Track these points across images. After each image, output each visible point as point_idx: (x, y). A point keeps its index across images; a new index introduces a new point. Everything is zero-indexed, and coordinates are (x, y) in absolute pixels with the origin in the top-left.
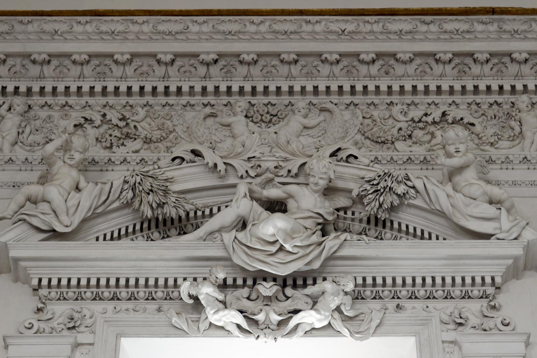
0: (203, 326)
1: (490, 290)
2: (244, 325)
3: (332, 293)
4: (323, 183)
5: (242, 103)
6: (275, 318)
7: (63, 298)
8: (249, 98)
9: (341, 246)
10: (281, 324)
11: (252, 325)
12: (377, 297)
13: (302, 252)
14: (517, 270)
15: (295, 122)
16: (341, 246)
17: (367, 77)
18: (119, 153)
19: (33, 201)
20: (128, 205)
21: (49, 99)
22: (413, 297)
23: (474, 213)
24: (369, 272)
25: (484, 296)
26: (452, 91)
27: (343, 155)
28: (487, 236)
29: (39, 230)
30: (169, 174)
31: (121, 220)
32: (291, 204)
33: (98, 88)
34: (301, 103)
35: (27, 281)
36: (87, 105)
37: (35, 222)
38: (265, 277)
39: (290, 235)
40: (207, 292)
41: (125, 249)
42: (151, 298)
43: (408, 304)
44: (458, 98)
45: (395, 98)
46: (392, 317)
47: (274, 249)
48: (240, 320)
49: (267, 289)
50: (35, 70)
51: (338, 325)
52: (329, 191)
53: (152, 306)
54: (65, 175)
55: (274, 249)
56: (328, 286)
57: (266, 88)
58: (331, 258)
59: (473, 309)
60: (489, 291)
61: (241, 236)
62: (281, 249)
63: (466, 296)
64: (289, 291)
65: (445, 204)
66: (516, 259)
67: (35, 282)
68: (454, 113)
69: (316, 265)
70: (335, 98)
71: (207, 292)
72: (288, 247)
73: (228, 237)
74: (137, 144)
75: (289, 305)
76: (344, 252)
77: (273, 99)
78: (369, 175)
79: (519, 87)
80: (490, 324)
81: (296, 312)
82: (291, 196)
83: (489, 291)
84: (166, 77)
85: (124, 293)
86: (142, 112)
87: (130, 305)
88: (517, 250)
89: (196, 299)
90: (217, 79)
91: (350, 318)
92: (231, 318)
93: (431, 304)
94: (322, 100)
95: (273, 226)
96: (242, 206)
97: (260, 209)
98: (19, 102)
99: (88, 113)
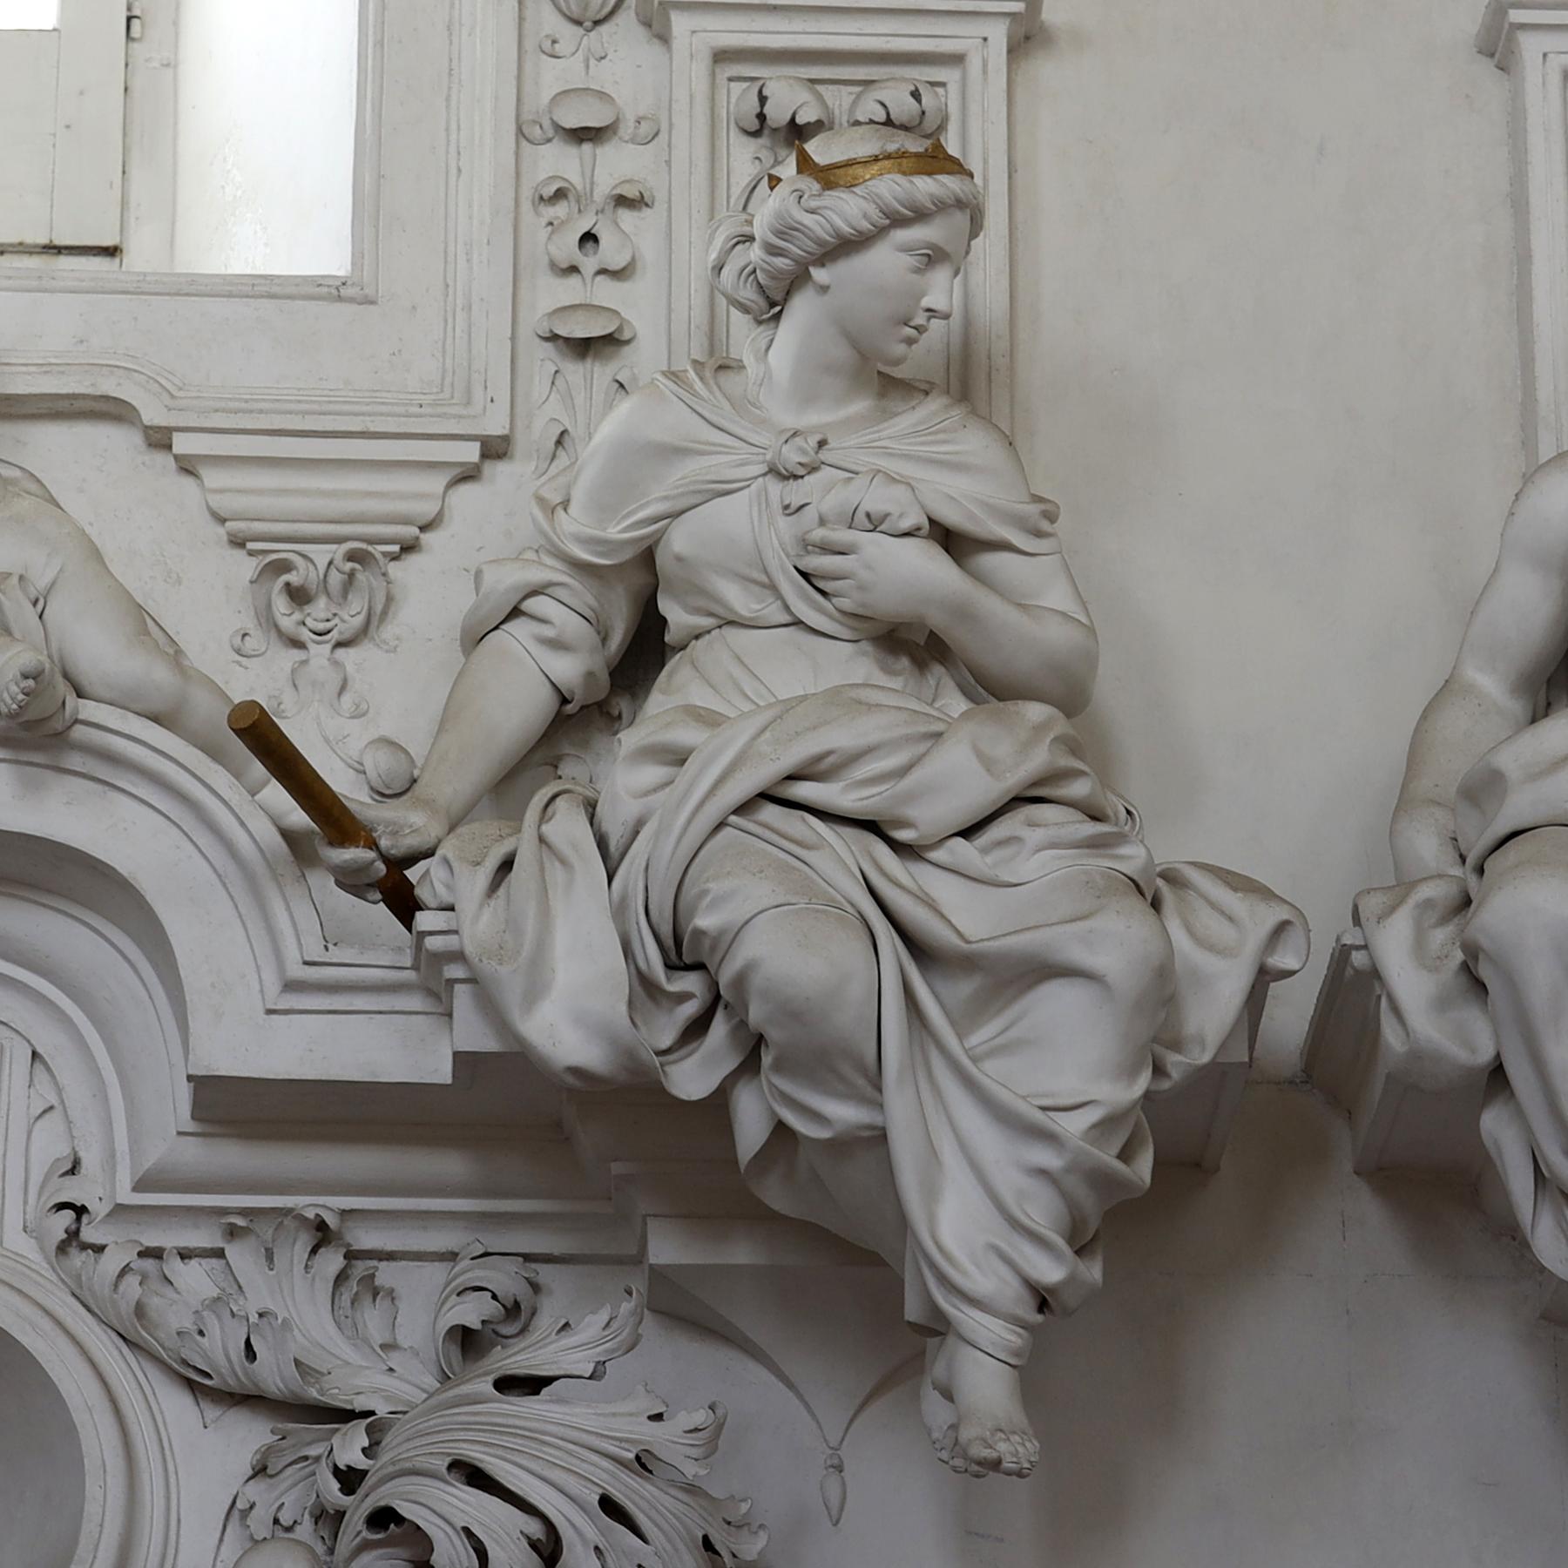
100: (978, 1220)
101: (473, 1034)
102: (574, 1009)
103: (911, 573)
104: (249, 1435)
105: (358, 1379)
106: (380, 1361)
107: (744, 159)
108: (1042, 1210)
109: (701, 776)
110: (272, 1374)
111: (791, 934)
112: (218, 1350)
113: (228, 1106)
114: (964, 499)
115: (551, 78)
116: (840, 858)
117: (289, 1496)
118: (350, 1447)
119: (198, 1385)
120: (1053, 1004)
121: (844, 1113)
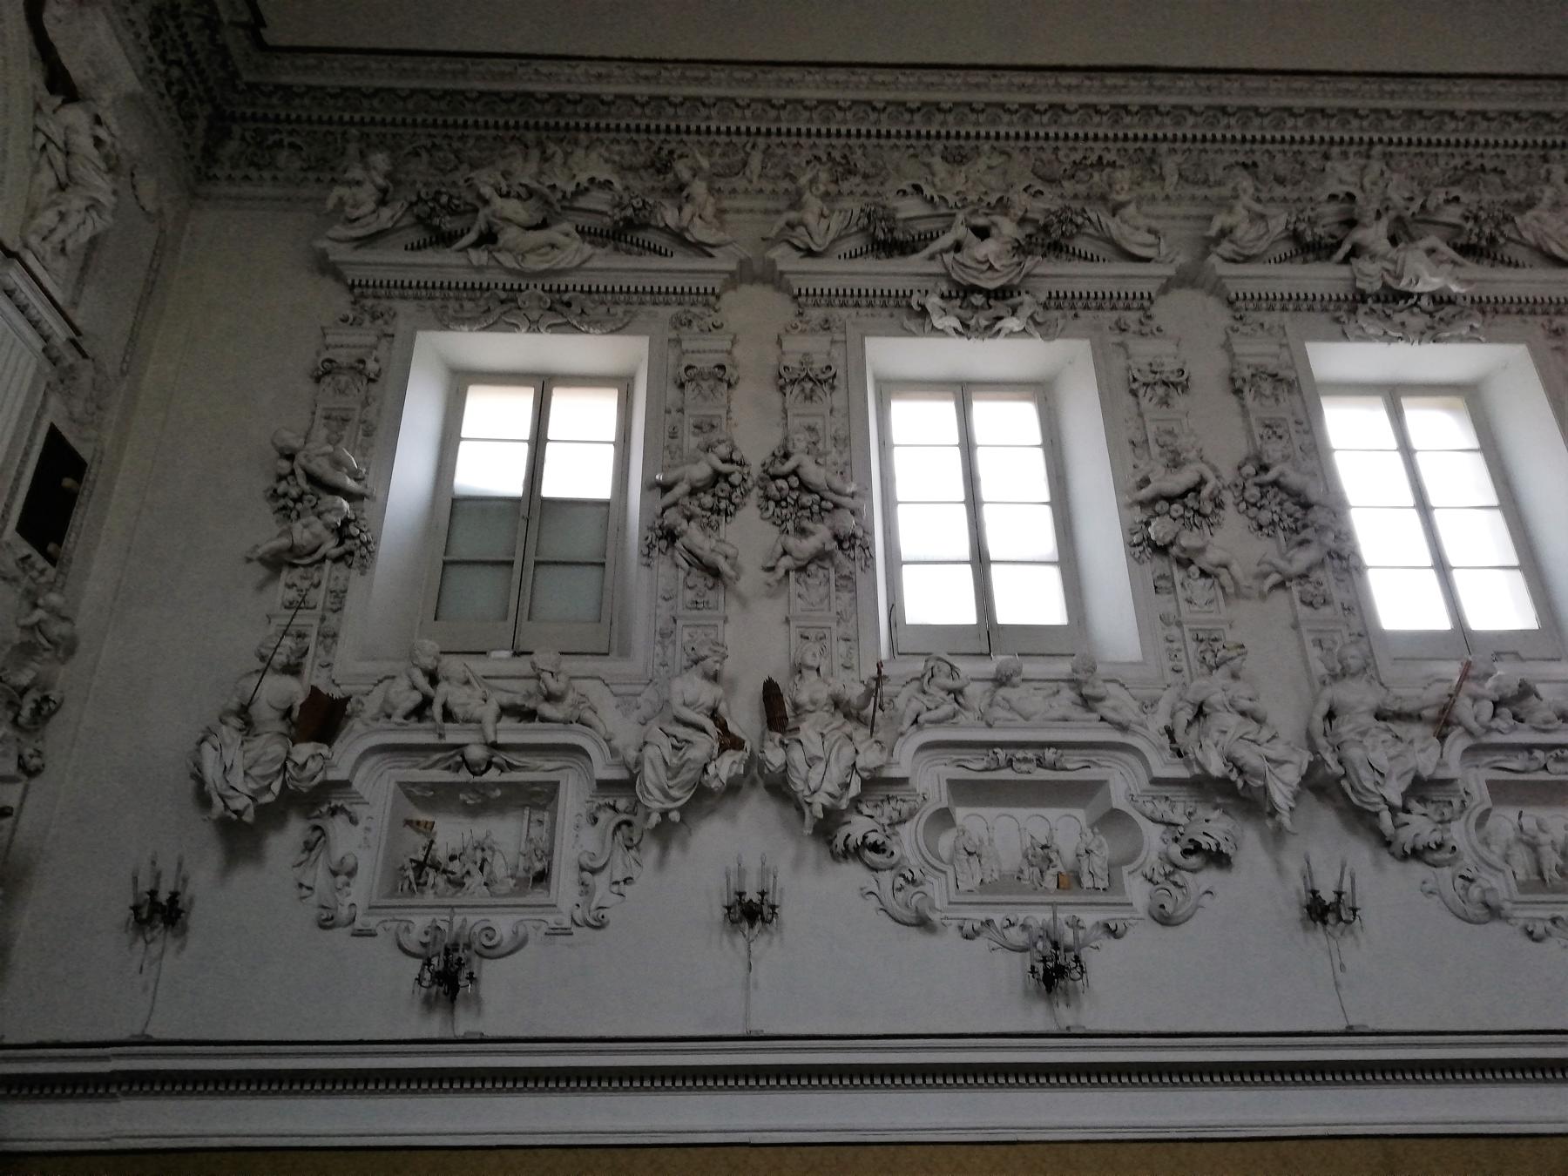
0: (928, 328)
1: (1146, 303)
2: (960, 328)
4: (1020, 213)
5: (939, 146)
6: (984, 323)
7: (817, 305)
10: (987, 328)
15: (982, 163)
16: (1035, 266)
17: (1041, 125)
18: (845, 186)
19: (791, 226)
20: (864, 229)
21: (784, 139)
22: (1086, 307)
23: (1136, 242)
25: (1142, 308)
27: (1032, 190)
28: (1148, 260)
29: (798, 248)
31: (854, 243)
32: (994, 231)
33: (824, 130)
34: (986, 147)
35: (788, 290)
37: (796, 242)
40: (933, 302)
41: (860, 265)
42: (884, 305)
43: (1082, 313)
44: (1110, 145)
49: (978, 300)
50: (773, 113)
51: (1032, 329)
52: (1022, 221)
53: (885, 312)
54: (813, 204)
55: (985, 267)
57: (859, 131)
58: (1028, 275)
59: (1132, 318)
61: (958, 256)
62: (991, 267)
63: (1128, 308)
64: (992, 302)
65: (1115, 233)
67: (796, 291)
71: (933, 302)
72: (997, 266)
73: (948, 258)
74: (858, 179)
75: (991, 313)
76: (1038, 271)
77: (962, 142)
78: (1054, 208)
80: (1146, 330)
81: (1000, 318)
82: (994, 224)
83: (1143, 304)
84: (878, 121)
85: (864, 302)
87: (869, 311)
88: (1170, 271)
89: (923, 307)
93: (1100, 313)
95: (988, 248)
96: (960, 231)
97: (971, 235)
98: (761, 141)
99: (816, 152)
100: (1281, 795)
101: (1197, 771)
102: (1216, 768)
103: (1245, 704)
104: (1162, 828)
105: (1176, 820)
106: (1178, 817)
107: (1194, 644)
108: (1290, 796)
109: (1229, 735)
110: (1166, 819)
111: (1250, 757)
112: (1157, 815)
113: (1156, 781)
115: (1166, 633)
116: (1254, 746)
117: (1169, 837)
118: (1181, 830)
119: (1153, 820)
120: (1286, 767)
121: (1260, 783)
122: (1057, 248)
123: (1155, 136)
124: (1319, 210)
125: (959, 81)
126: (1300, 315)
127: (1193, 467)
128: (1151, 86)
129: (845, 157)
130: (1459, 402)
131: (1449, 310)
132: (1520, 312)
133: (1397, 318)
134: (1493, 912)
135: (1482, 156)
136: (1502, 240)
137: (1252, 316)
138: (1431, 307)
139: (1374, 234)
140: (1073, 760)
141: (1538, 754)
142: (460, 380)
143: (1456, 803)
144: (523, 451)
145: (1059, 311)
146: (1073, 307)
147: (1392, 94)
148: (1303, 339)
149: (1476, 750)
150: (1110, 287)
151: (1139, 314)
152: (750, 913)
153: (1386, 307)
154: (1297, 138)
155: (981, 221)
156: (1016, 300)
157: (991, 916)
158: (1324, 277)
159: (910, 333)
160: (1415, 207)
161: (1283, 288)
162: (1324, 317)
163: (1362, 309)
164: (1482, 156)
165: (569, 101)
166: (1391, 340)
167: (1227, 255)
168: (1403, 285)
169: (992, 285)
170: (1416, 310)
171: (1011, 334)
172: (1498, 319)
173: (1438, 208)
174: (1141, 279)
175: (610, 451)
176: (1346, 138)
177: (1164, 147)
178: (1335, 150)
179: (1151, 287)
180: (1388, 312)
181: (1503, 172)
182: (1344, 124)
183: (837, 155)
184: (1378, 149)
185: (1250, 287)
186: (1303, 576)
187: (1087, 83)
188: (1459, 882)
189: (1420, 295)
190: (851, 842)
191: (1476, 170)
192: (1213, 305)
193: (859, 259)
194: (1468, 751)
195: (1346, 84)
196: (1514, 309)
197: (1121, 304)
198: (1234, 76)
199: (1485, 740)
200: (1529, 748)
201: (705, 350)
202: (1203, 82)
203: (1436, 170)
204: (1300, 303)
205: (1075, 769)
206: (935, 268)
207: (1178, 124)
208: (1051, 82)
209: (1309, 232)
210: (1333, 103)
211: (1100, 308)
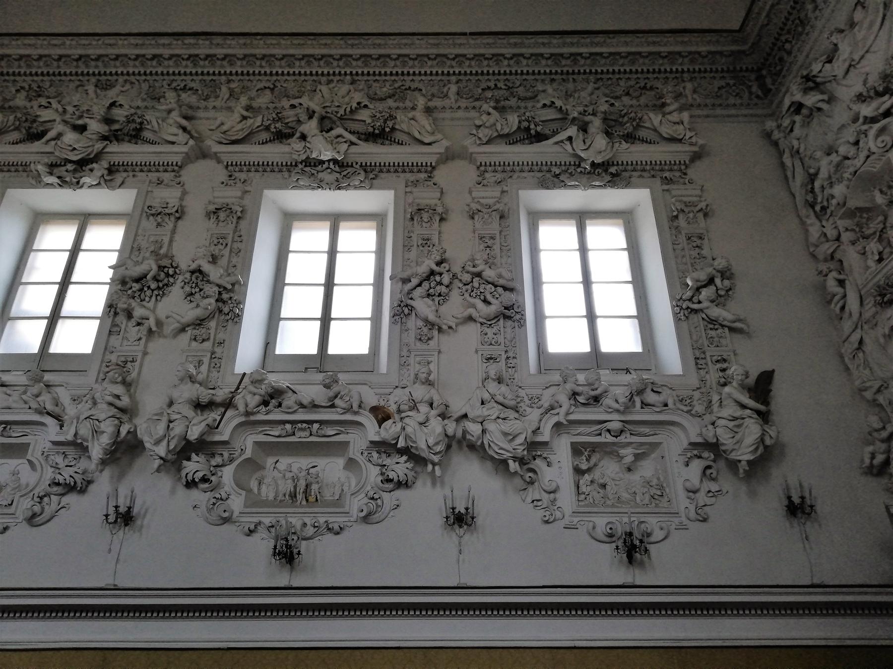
1: (176, 168)
3: (99, 169)
5: (93, 80)
8: (97, 77)
9: (103, 149)
11: (63, 183)
12: (125, 171)
13: (84, 150)
14: (188, 159)
22: (142, 171)
24: (116, 159)
25: (173, 171)
26: (191, 74)
28: (173, 143)
30: (38, 113)
34: (121, 79)
36: (24, 81)
38: (71, 162)
39: (78, 141)
45: (166, 77)
46: (130, 180)
47: (71, 148)
48: (57, 180)
49: (70, 167)
56: (94, 165)
59: (167, 177)
60: (177, 169)
61: (59, 143)
63: (166, 171)
66: (187, 153)
68: (192, 85)
69: (92, 156)
70: (138, 77)
73: (53, 143)
77: (109, 78)
79: (222, 72)
86: (48, 84)
87: (16, 174)
90: (83, 69)
91: (111, 180)
92: (53, 180)
93: (150, 174)
94: (132, 78)
103: (110, 399)
108: (101, 452)
113: (55, 443)
114: (117, 392)
122: (136, 135)
123: (220, 72)
124: (285, 113)
125: (100, 42)
126: (265, 174)
127: (146, 262)
128: (211, 43)
129: (39, 87)
130: (621, 221)
131: (349, 170)
132: (396, 171)
133: (321, 175)
134: (226, 521)
135: (413, 80)
136: (387, 130)
137: (237, 174)
138: (337, 169)
139: (311, 127)
140: (17, 431)
141: (288, 426)
142: (289, 220)
143: (226, 454)
144: (324, 258)
145: (113, 175)
146: (134, 171)
147: (352, 46)
148: (139, 189)
149: (248, 424)
150: (153, 159)
151: (173, 174)
152: (126, 518)
153: (309, 171)
154: (303, 72)
155: (80, 122)
156: (90, 166)
157: (263, 520)
158: (276, 152)
159: (33, 187)
160: (342, 112)
161: (253, 159)
162: (279, 175)
163: (298, 169)
164: (413, 80)
165: (238, 59)
166: (313, 189)
167: (217, 139)
168: (314, 156)
169: (75, 158)
170: (329, 170)
171: (91, 186)
172: (383, 175)
173: (352, 111)
174: (174, 154)
175: (372, 257)
176: (331, 72)
177: (223, 78)
178: (324, 79)
179: (178, 159)
180: (313, 172)
181: (421, 90)
182: (328, 64)
183: (34, 86)
184: (348, 77)
185: (236, 159)
186: (199, 323)
187: (175, 42)
188: (214, 501)
189: (329, 161)
190: (190, 478)
191: (406, 89)
192: (220, 167)
193: (19, 145)
194: (241, 425)
195: (324, 40)
196: (392, 169)
197: (161, 169)
198: (259, 37)
199: (252, 418)
200: (284, 422)
201: (426, 196)
202: (242, 41)
203: (385, 89)
204: (264, 167)
205: (15, 437)
206: (48, 149)
207: (673, 63)
208: (153, 42)
209: (273, 126)
210: (318, 52)
211: (150, 171)
